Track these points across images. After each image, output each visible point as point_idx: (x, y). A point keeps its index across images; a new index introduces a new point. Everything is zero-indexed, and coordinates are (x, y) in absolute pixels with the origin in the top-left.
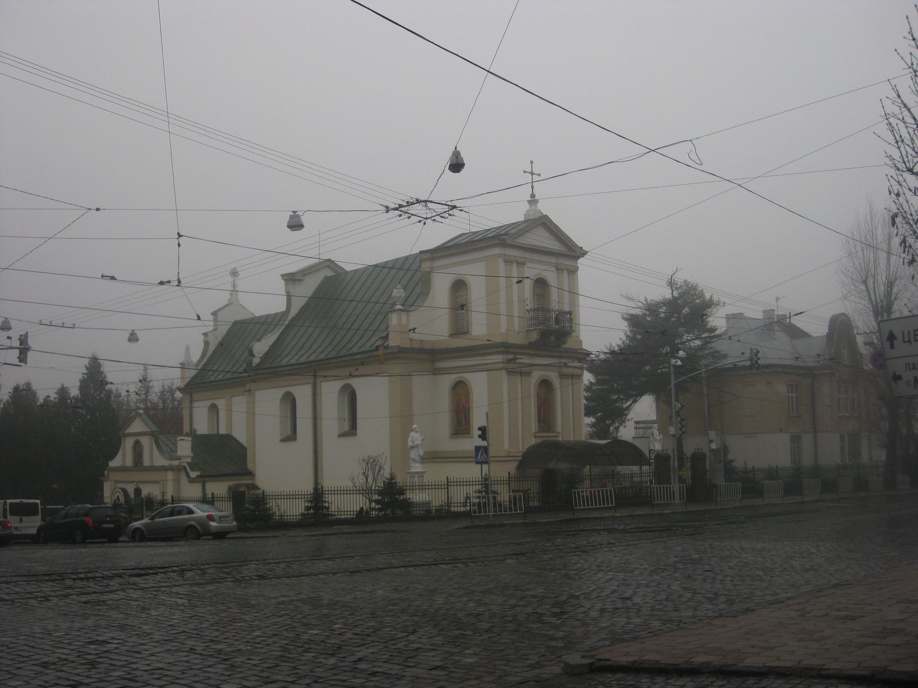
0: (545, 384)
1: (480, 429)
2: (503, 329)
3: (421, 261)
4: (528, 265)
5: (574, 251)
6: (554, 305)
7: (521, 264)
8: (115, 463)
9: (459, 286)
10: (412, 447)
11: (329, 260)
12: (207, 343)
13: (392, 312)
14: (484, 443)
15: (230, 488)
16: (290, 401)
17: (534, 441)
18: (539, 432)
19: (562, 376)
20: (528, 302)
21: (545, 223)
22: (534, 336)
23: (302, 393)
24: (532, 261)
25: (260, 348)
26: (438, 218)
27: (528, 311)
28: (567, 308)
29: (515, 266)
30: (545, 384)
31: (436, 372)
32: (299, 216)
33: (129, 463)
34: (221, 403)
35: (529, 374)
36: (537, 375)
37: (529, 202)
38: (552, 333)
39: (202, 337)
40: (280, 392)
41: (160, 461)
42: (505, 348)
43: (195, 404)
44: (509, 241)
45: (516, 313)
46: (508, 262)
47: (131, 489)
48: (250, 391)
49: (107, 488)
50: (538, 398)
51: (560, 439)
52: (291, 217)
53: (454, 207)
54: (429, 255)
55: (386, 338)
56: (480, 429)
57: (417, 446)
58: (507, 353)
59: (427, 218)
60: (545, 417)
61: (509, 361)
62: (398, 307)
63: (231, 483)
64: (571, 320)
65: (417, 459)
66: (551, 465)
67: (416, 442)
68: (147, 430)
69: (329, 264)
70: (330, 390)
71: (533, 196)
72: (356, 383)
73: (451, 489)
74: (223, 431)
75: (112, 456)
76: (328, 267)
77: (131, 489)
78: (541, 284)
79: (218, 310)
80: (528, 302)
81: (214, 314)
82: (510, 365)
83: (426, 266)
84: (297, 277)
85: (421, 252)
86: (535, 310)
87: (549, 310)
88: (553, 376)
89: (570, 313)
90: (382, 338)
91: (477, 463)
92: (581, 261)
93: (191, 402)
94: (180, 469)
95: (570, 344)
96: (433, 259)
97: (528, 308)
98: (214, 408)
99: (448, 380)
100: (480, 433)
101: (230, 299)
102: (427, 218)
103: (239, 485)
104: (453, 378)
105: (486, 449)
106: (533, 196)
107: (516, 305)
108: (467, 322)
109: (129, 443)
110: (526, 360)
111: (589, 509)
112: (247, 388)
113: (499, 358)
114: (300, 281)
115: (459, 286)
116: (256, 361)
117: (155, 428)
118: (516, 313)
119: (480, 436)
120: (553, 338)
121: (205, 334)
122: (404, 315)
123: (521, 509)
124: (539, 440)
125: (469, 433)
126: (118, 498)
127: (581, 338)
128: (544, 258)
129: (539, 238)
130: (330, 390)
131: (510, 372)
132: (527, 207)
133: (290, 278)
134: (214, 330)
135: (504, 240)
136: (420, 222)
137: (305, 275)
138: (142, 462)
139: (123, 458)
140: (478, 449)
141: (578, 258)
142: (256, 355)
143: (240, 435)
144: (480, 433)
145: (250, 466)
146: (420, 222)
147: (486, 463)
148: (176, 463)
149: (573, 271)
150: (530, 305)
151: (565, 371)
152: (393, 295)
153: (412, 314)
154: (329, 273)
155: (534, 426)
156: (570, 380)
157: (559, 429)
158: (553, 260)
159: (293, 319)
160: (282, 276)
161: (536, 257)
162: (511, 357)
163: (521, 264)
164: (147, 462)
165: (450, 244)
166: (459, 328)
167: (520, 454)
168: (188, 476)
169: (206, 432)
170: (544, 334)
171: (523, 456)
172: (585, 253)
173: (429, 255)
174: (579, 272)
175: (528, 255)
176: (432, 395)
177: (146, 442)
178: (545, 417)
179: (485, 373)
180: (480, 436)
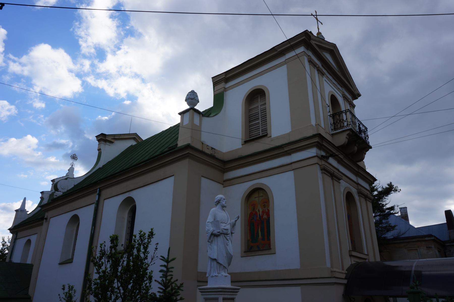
2: (313, 122)
10: (214, 235)
11: (136, 134)
12: (42, 198)
31: (226, 183)
39: (40, 195)
57: (224, 234)
67: (223, 226)
74: (29, 262)
76: (134, 139)
98: (29, 242)
99: (241, 190)
104: (245, 187)
113: (313, 152)
114: (112, 142)
125: (270, 249)
133: (103, 138)
137: (115, 139)
142: (60, 189)
159: (100, 168)
162: (324, 154)
169: (19, 262)
179: (292, 173)
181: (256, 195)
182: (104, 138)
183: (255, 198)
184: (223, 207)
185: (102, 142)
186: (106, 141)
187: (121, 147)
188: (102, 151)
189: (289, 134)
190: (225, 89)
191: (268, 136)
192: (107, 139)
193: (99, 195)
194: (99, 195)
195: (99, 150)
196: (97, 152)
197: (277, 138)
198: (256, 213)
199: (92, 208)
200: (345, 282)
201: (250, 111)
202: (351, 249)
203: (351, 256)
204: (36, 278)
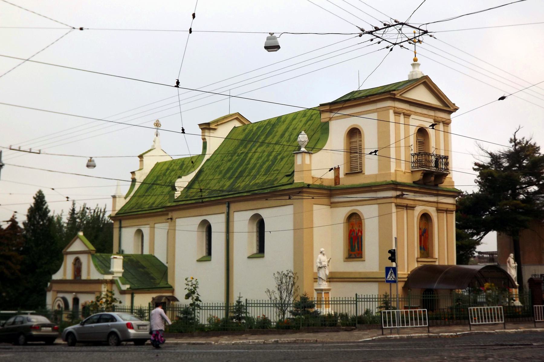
0: (425, 217)
1: (390, 252)
2: (393, 170)
3: (322, 112)
4: (412, 116)
5: (449, 107)
6: (432, 150)
7: (407, 115)
8: (56, 277)
9: (354, 133)
12: (134, 181)
13: (297, 153)
14: (394, 265)
15: (153, 299)
16: (208, 228)
17: (416, 265)
18: (421, 257)
19: (439, 210)
20: (412, 147)
21: (426, 82)
22: (418, 176)
23: (217, 222)
24: (416, 113)
25: (182, 183)
26: (406, 44)
27: (413, 156)
28: (442, 153)
29: (402, 116)
30: (425, 217)
31: (332, 205)
32: (275, 38)
33: (70, 276)
34: (146, 230)
35: (412, 208)
36: (419, 210)
37: (413, 65)
38: (431, 175)
40: (200, 219)
41: (96, 275)
42: (394, 186)
43: (123, 230)
44: (398, 96)
45: (403, 158)
46: (397, 113)
47: (70, 298)
48: (171, 219)
49: (50, 298)
50: (420, 229)
51: (437, 264)
52: (268, 39)
53: (426, 32)
54: (327, 108)
55: (291, 175)
56: (390, 252)
58: (396, 190)
59: (395, 44)
60: (425, 247)
61: (397, 197)
62: (303, 149)
63: (155, 295)
64: (447, 164)
65: (324, 277)
66: (435, 286)
67: (324, 264)
68: (86, 249)
69: (238, 117)
70: (242, 219)
71: (415, 60)
72: (265, 214)
73: (360, 304)
74: (146, 252)
75: (55, 271)
77: (70, 298)
78: (422, 132)
79: (144, 154)
80: (412, 147)
81: (141, 157)
82: (399, 201)
83: (325, 116)
84: (212, 126)
85: (321, 105)
86: (418, 154)
87: (429, 155)
88: (432, 211)
89: (446, 158)
90: (287, 176)
91: (387, 281)
92: (453, 115)
93: (120, 228)
94: (112, 282)
95: (445, 184)
96: (331, 111)
97: (413, 152)
98: (139, 232)
99: (343, 212)
100: (390, 255)
101: (154, 146)
102: (395, 44)
103: (161, 297)
105: (395, 270)
106: (415, 60)
107: (403, 149)
108: (361, 164)
109: (69, 261)
110: (411, 195)
111: (495, 324)
112: (169, 217)
114: (215, 129)
115: (354, 133)
116: (177, 194)
117: (92, 248)
118: (403, 158)
119: (390, 258)
120: (433, 178)
121: (133, 173)
122: (307, 156)
123: (425, 324)
124: (420, 265)
125: (361, 257)
126: (59, 306)
127: (453, 180)
128: (425, 111)
129: (421, 94)
130: (242, 219)
131: (397, 206)
132: (411, 68)
133: (206, 127)
134: (140, 170)
135: (395, 95)
136: (387, 48)
137: (218, 125)
138: (80, 276)
139: (65, 272)
140: (388, 269)
141: (450, 112)
143: (161, 255)
144: (390, 255)
145: (170, 282)
146: (387, 48)
147: (395, 282)
148: (109, 277)
149: (447, 123)
150: (414, 150)
151: (440, 206)
152: (299, 139)
153: (313, 156)
154: (237, 124)
155: (416, 253)
156: (445, 214)
157: (437, 256)
158: (432, 113)
159: (208, 160)
160: (200, 125)
161: (419, 110)
162: (399, 193)
163: (407, 115)
164: (84, 277)
165: (347, 98)
166: (355, 168)
167: (406, 276)
168: (119, 288)
170: (426, 175)
171: (407, 277)
172: (456, 109)
173: (327, 108)
174: (452, 125)
175: (413, 109)
176: (327, 224)
177: (84, 259)
178: (425, 247)
179: (377, 206)
180: (390, 258)
181: (354, 217)
182: (208, 127)
183: (353, 220)
184: (324, 254)
185: (206, 131)
186: (210, 129)
187: (224, 131)
188: (207, 140)
189: (376, 175)
190: (331, 119)
191: (363, 172)
192: (211, 127)
193: (229, 207)
194: (229, 207)
195: (204, 139)
196: (202, 141)
197: (369, 176)
198: (354, 231)
199: (222, 218)
200: (406, 280)
201: (351, 143)
202: (419, 257)
203: (418, 261)
204: (174, 272)
